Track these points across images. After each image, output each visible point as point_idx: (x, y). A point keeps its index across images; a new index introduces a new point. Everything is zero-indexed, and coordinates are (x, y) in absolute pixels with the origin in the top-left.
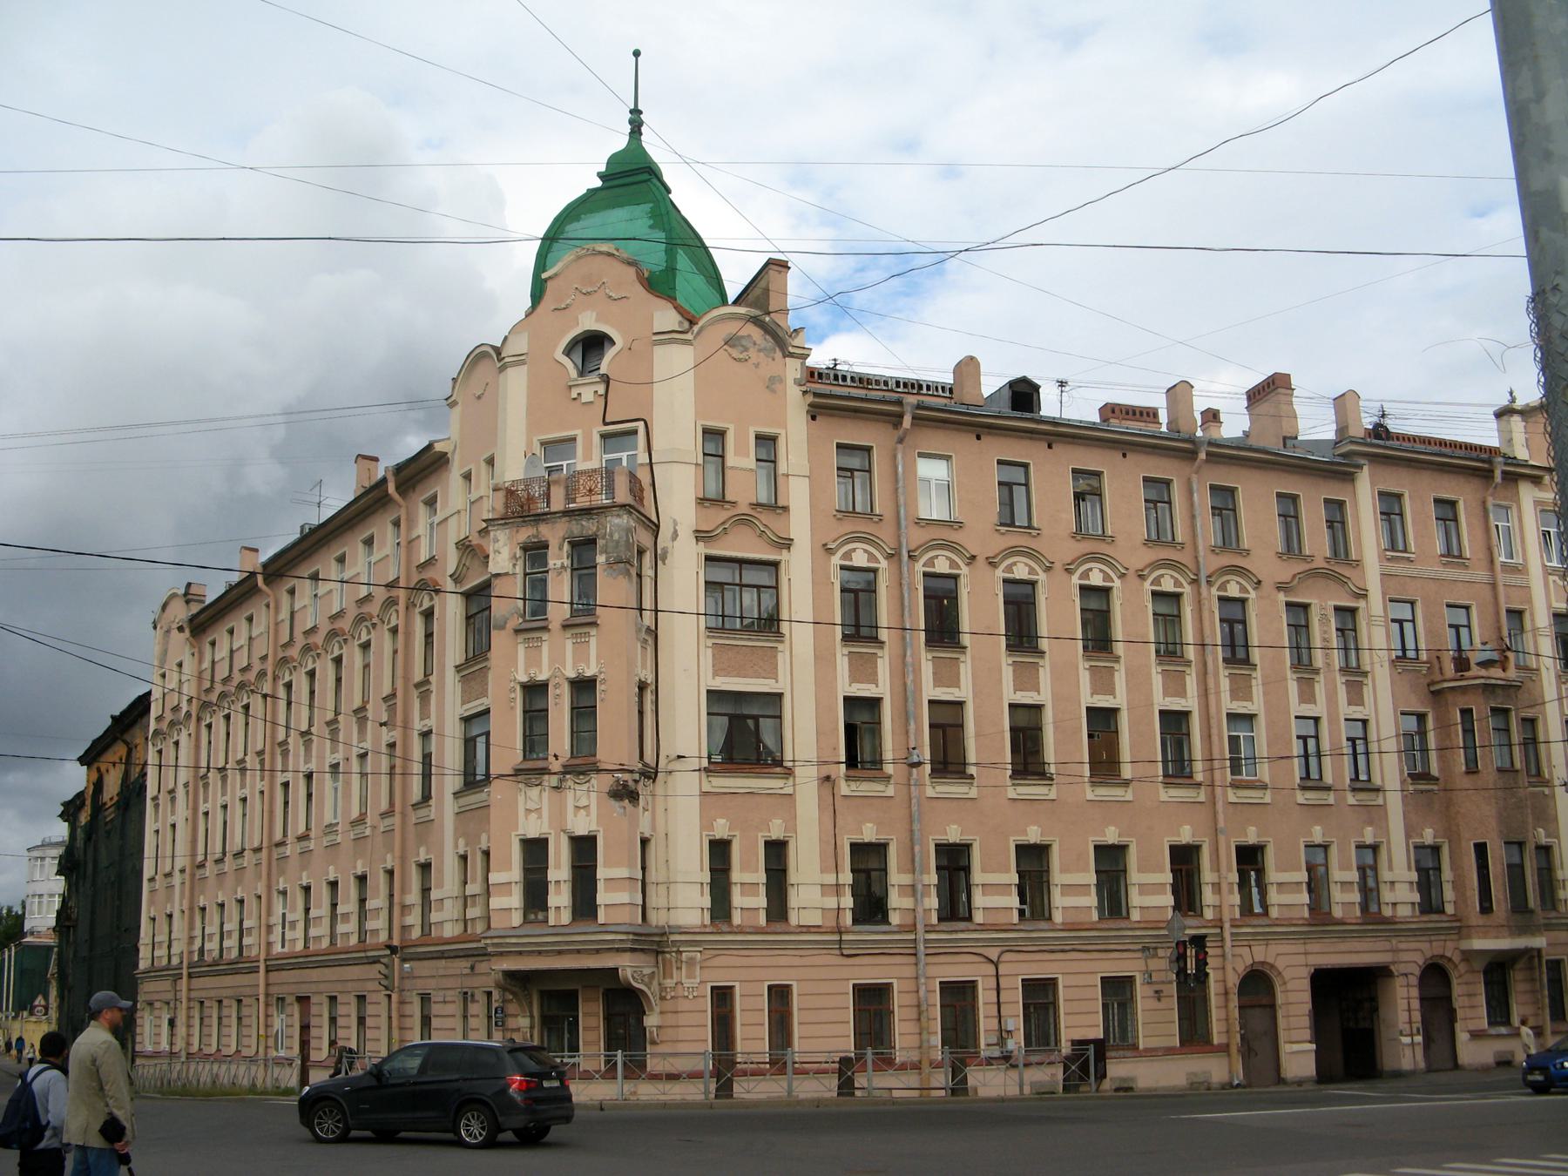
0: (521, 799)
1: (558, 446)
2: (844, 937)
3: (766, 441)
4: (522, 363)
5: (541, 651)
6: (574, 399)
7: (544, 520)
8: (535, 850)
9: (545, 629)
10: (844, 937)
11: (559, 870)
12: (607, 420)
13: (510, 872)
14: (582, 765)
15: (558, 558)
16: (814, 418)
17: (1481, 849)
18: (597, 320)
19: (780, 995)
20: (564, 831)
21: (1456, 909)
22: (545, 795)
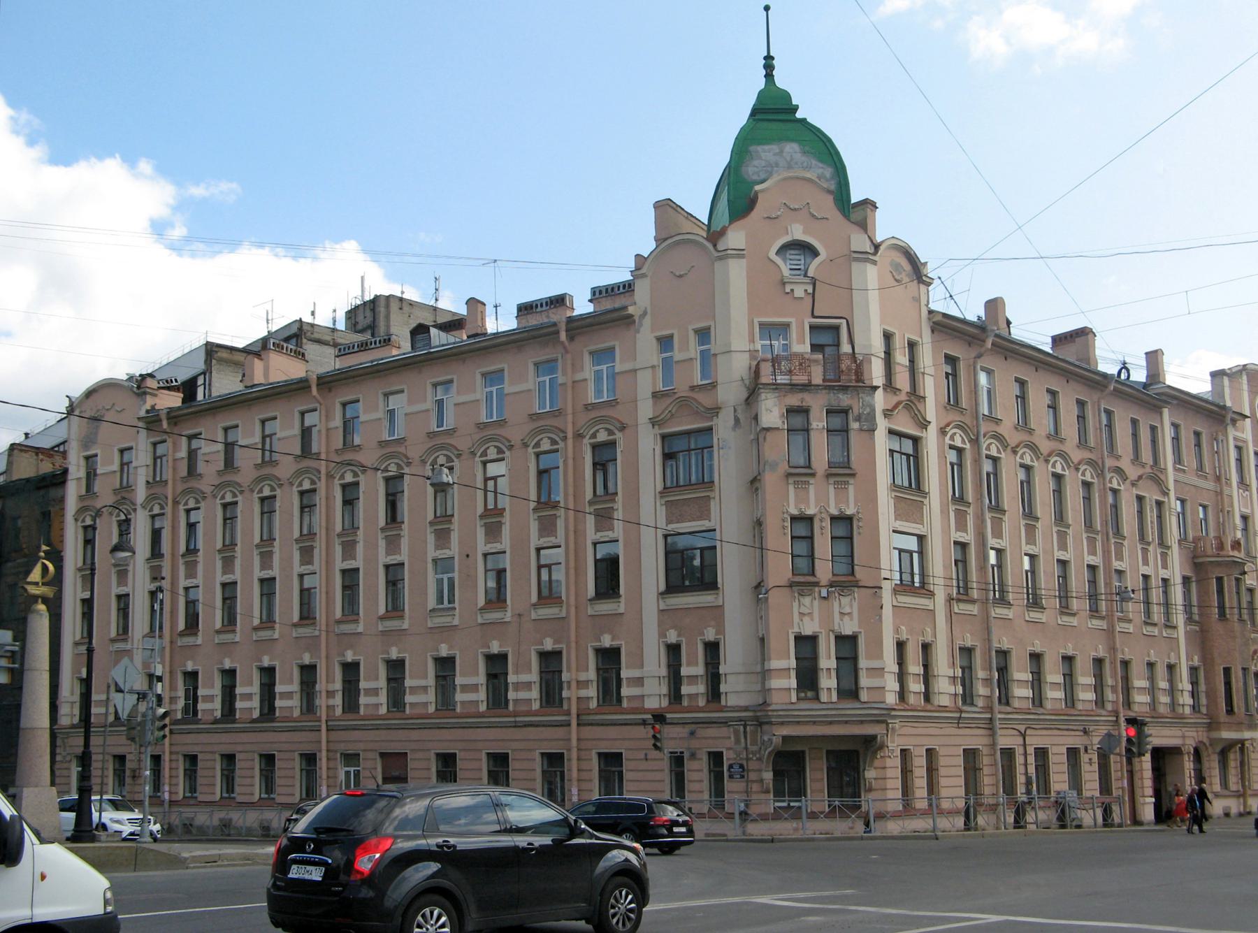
0: (796, 604)
1: (773, 330)
2: (963, 715)
3: (912, 345)
4: (742, 256)
5: (808, 493)
6: (788, 293)
7: (807, 390)
8: (807, 644)
9: (813, 475)
10: (963, 715)
11: (827, 661)
12: (816, 314)
13: (785, 661)
14: (846, 582)
15: (819, 422)
16: (933, 331)
17: (1227, 671)
18: (804, 232)
19: (930, 753)
20: (833, 631)
21: (1207, 711)
22: (816, 603)
